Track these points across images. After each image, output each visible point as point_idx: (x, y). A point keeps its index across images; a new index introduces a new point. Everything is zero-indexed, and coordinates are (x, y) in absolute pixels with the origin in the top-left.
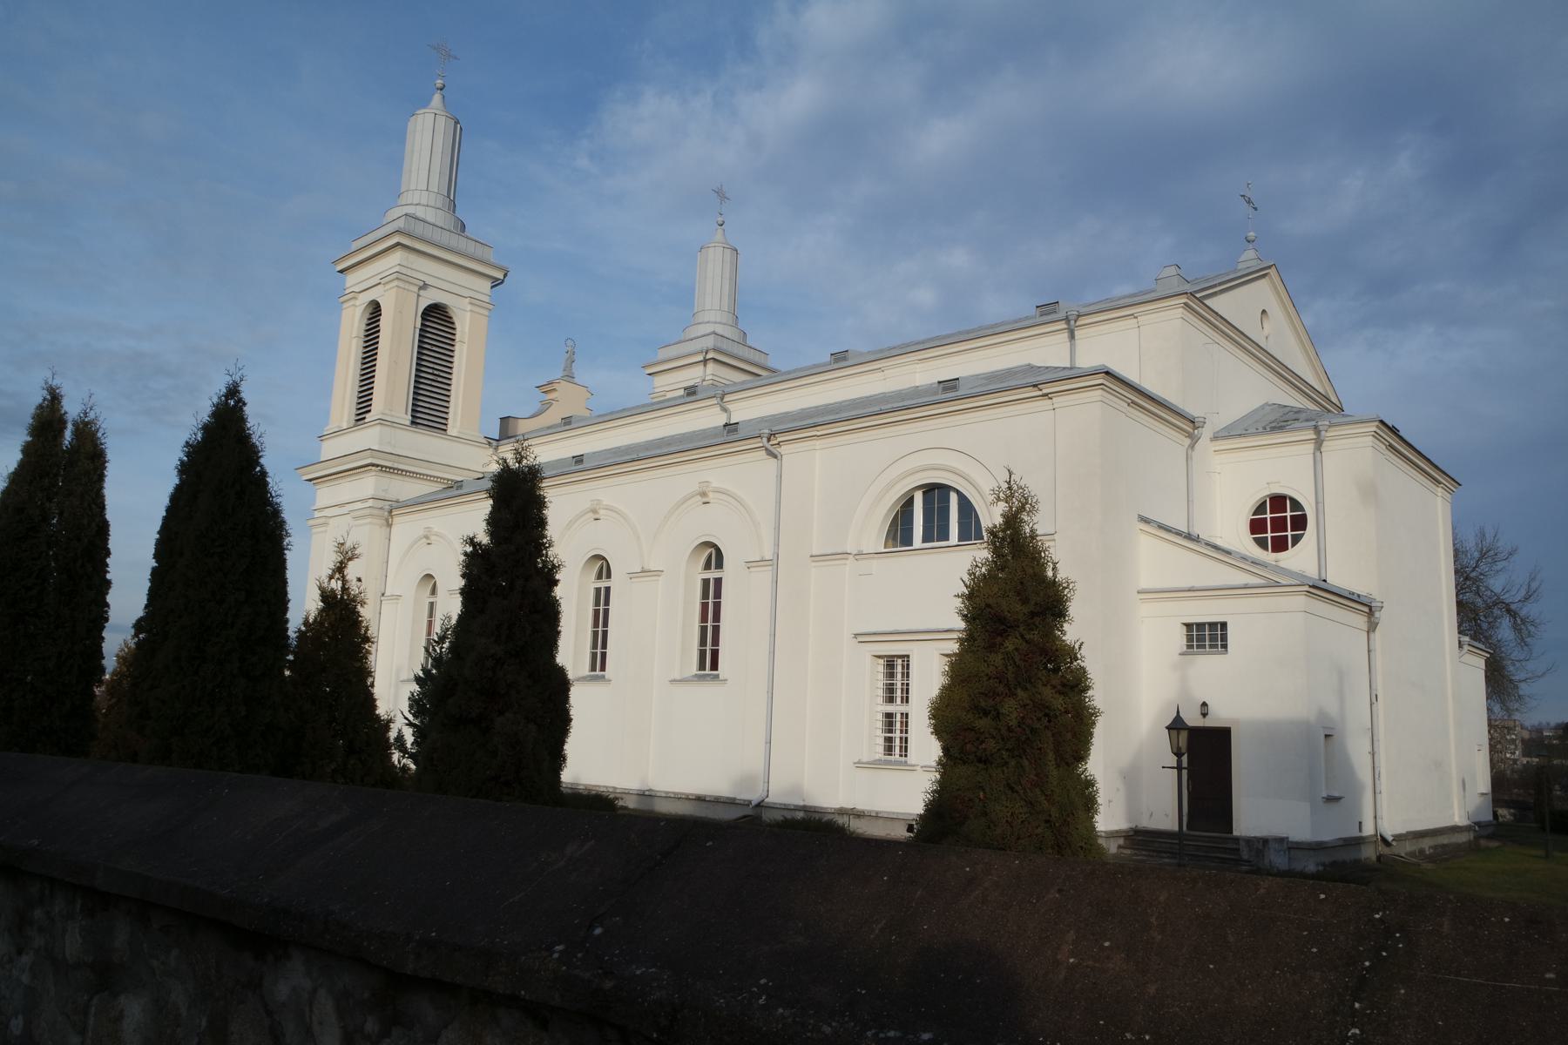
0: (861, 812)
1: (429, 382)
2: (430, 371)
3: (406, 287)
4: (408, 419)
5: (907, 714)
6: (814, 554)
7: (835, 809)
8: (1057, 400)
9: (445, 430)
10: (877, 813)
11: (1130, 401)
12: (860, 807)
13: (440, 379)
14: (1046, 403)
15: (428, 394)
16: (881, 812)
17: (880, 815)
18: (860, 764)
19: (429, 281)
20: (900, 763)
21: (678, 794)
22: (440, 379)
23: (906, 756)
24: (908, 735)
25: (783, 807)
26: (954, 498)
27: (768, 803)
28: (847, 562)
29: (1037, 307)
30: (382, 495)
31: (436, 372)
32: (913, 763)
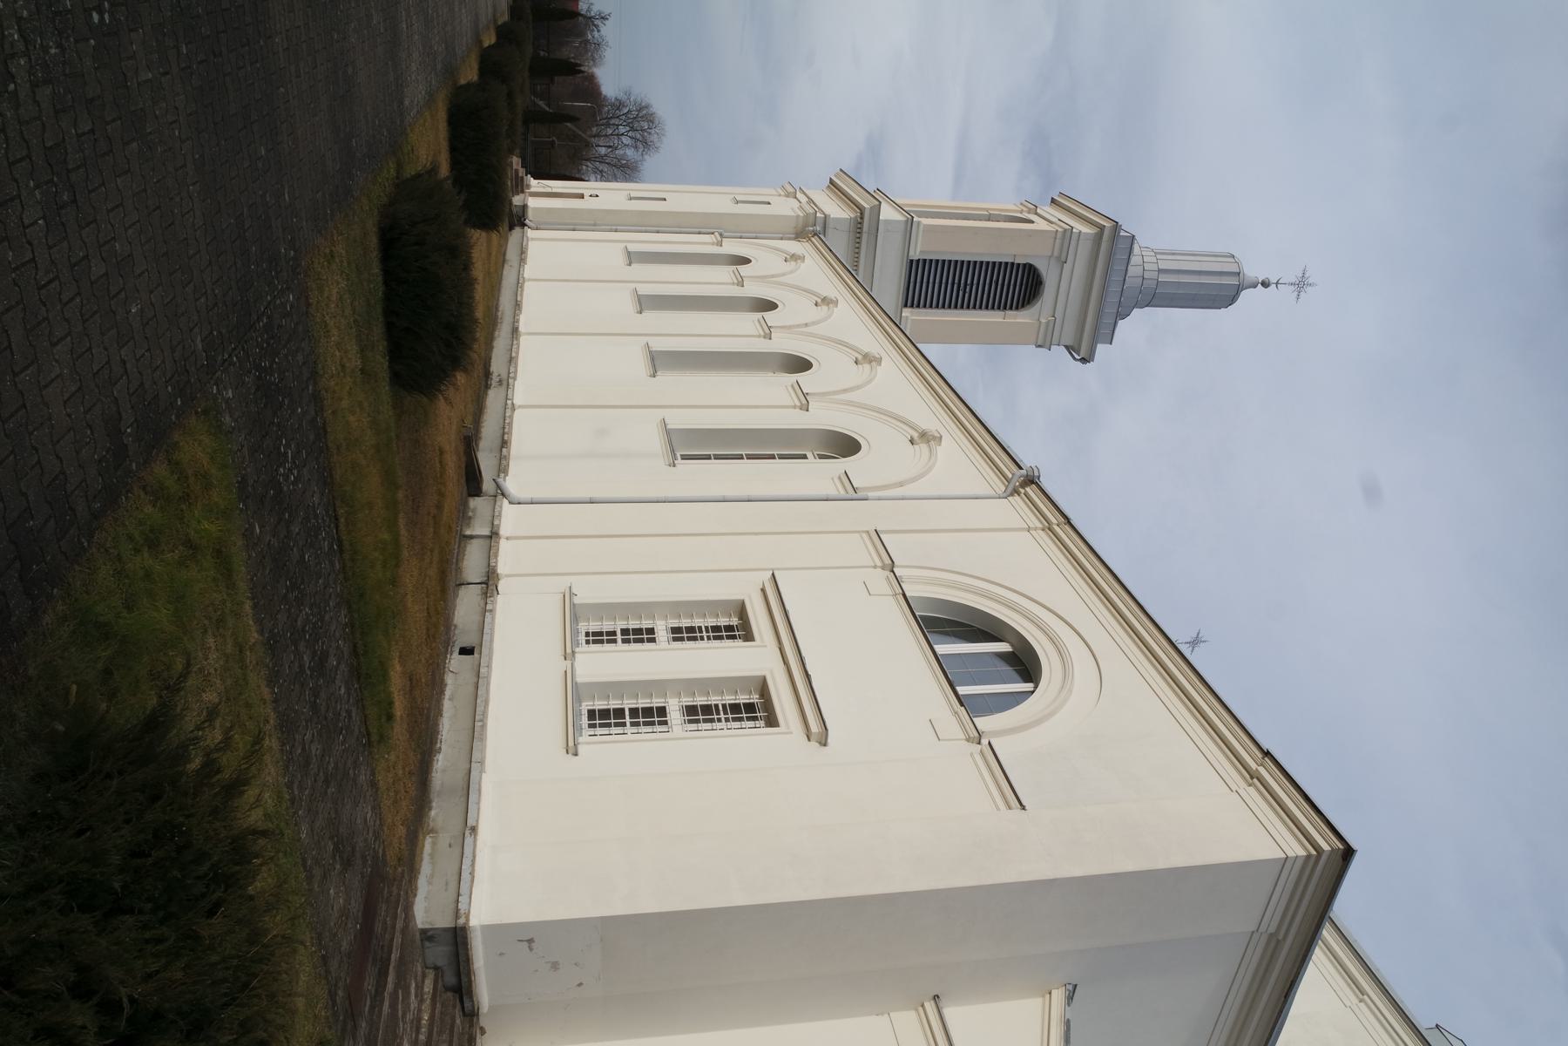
1: (956, 281)
2: (969, 282)
3: (1057, 240)
4: (915, 254)
5: (653, 640)
9: (906, 306)
11: (1280, 937)
13: (961, 293)
15: (937, 281)
16: (493, 619)
19: (1067, 267)
20: (575, 632)
21: (510, 424)
22: (961, 293)
23: (588, 642)
25: (497, 514)
26: (1028, 686)
27: (502, 504)
30: (830, 225)
31: (968, 287)
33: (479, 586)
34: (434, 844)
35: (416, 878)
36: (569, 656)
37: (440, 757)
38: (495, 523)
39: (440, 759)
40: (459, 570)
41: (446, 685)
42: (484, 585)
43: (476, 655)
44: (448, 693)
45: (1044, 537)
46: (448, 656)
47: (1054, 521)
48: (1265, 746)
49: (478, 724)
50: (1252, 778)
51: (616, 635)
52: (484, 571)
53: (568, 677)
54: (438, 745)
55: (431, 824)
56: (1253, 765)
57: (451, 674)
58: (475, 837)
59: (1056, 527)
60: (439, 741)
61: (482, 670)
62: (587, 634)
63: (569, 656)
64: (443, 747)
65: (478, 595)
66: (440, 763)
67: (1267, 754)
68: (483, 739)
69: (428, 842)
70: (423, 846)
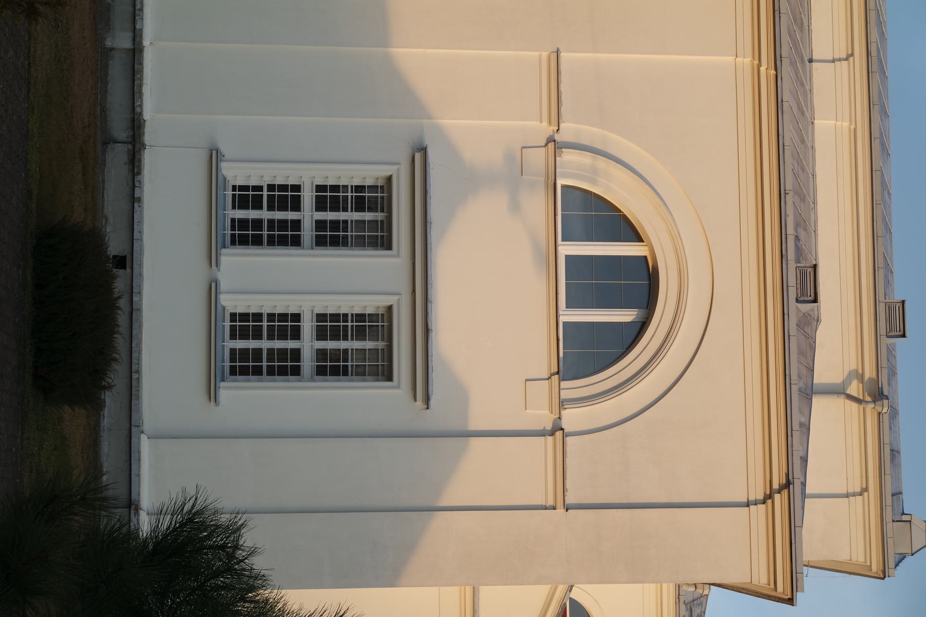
0: (139, 167)
6: (563, 55)
7: (141, 114)
10: (139, 200)
12: (148, 159)
17: (136, 205)
18: (214, 157)
24: (266, 310)
28: (545, 124)
29: (903, 302)
32: (224, 260)
36: (213, 260)
37: (106, 412)
38: (138, 27)
39: (106, 415)
42: (130, 146)
43: (128, 270)
49: (135, 376)
53: (212, 289)
61: (135, 299)
62: (234, 188)
63: (213, 260)
65: (125, 164)
66: (106, 420)
68: (138, 397)
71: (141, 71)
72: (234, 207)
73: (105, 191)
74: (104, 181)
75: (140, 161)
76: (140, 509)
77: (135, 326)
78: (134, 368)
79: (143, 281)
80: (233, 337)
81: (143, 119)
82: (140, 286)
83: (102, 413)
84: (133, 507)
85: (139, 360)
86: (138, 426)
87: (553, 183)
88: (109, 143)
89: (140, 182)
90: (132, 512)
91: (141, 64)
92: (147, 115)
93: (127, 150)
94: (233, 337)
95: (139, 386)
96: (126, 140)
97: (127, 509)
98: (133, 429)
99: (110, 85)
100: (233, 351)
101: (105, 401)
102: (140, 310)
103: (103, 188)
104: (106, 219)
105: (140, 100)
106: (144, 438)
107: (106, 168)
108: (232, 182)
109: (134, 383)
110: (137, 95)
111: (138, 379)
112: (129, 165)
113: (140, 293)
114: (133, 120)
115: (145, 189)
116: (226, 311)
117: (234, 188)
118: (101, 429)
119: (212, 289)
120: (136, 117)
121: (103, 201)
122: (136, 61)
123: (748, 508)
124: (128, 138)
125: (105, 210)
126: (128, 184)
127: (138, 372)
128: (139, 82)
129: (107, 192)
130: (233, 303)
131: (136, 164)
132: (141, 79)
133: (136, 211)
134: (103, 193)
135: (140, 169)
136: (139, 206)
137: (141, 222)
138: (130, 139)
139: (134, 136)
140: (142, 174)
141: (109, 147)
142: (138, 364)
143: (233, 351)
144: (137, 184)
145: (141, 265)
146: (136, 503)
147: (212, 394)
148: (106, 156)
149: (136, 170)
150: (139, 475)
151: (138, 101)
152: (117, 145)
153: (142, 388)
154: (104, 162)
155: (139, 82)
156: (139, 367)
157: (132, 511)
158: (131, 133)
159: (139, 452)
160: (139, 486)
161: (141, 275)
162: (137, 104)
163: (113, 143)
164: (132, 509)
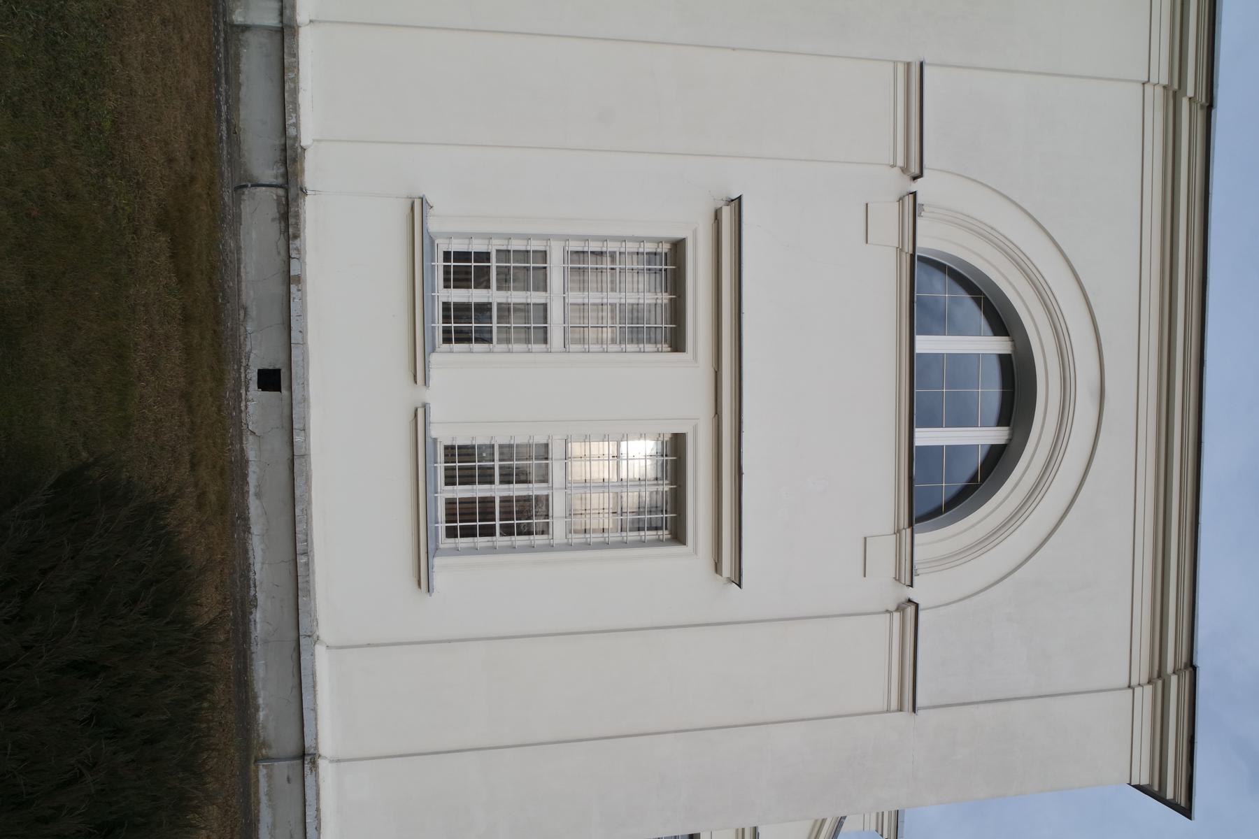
7: (296, 138)
8: (1145, 695)
10: (298, 279)
12: (311, 211)
14: (1142, 671)
17: (293, 288)
18: (418, 209)
33: (274, 190)
34: (270, 777)
35: (256, 830)
36: (418, 373)
37: (258, 615)
39: (258, 620)
40: (236, 160)
41: (247, 462)
42: (281, 192)
43: (285, 392)
44: (252, 480)
45: (1156, 97)
46: (243, 391)
47: (1190, 93)
48: (1200, 661)
49: (302, 560)
50: (1159, 676)
51: (488, 260)
52: (277, 143)
53: (419, 416)
54: (252, 593)
55: (262, 734)
56: (1170, 667)
57: (251, 438)
58: (317, 775)
59: (1185, 102)
60: (253, 623)
61: (297, 439)
62: (447, 255)
63: (418, 373)
64: (261, 597)
65: (273, 220)
66: (258, 626)
67: (1192, 667)
68: (308, 592)
69: (262, 772)
70: (258, 781)
71: (296, 67)
72: (447, 286)
73: (242, 266)
74: (239, 248)
75: (297, 216)
76: (320, 756)
77: (299, 481)
78: (300, 547)
79: (309, 407)
80: (450, 481)
81: (302, 147)
82: (305, 418)
83: (251, 617)
84: (308, 758)
85: (307, 535)
86: (309, 636)
87: (911, 252)
88: (246, 186)
89: (297, 250)
90: (307, 767)
91: (295, 55)
92: (305, 140)
93: (275, 197)
94: (450, 481)
95: (308, 575)
96: (274, 181)
97: (299, 762)
98: (302, 641)
99: (243, 89)
100: (450, 503)
101: (256, 599)
102: (305, 456)
103: (239, 260)
104: (245, 309)
105: (294, 115)
106: (320, 650)
107: (242, 227)
108: (443, 246)
109: (301, 570)
110: (289, 107)
111: (307, 564)
112: (280, 223)
113: (304, 430)
114: (284, 149)
115: (308, 260)
116: (439, 443)
117: (447, 255)
118: (253, 640)
119: (419, 416)
120: (289, 142)
121: (239, 282)
122: (286, 50)
123: (1131, 691)
124: (276, 177)
125: (244, 297)
126: (279, 253)
127: (305, 553)
128: (292, 86)
129: (245, 267)
130: (446, 432)
131: (292, 221)
132: (295, 81)
133: (294, 298)
134: (239, 268)
135: (299, 230)
136: (299, 290)
137: (303, 315)
138: (280, 181)
139: (286, 175)
140: (302, 238)
141: (246, 193)
142: (306, 541)
143: (450, 503)
144: (293, 254)
145: (305, 385)
146: (312, 751)
147: (423, 579)
148: (242, 206)
149: (291, 230)
150: (314, 710)
151: (291, 116)
152: (259, 189)
153: (314, 573)
154: (238, 217)
155: (292, 86)
156: (307, 545)
157: (305, 766)
158: (282, 170)
159: (314, 674)
160: (316, 724)
161: (305, 400)
162: (290, 121)
163: (252, 186)
164: (306, 762)
